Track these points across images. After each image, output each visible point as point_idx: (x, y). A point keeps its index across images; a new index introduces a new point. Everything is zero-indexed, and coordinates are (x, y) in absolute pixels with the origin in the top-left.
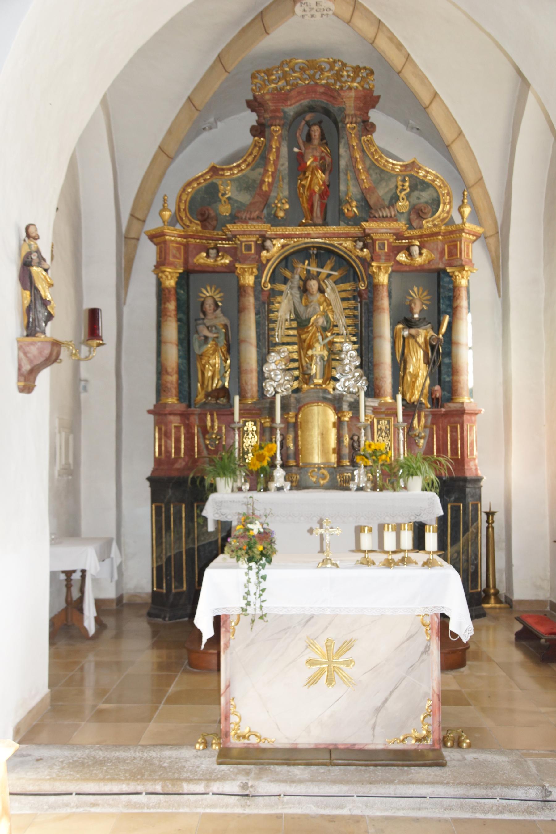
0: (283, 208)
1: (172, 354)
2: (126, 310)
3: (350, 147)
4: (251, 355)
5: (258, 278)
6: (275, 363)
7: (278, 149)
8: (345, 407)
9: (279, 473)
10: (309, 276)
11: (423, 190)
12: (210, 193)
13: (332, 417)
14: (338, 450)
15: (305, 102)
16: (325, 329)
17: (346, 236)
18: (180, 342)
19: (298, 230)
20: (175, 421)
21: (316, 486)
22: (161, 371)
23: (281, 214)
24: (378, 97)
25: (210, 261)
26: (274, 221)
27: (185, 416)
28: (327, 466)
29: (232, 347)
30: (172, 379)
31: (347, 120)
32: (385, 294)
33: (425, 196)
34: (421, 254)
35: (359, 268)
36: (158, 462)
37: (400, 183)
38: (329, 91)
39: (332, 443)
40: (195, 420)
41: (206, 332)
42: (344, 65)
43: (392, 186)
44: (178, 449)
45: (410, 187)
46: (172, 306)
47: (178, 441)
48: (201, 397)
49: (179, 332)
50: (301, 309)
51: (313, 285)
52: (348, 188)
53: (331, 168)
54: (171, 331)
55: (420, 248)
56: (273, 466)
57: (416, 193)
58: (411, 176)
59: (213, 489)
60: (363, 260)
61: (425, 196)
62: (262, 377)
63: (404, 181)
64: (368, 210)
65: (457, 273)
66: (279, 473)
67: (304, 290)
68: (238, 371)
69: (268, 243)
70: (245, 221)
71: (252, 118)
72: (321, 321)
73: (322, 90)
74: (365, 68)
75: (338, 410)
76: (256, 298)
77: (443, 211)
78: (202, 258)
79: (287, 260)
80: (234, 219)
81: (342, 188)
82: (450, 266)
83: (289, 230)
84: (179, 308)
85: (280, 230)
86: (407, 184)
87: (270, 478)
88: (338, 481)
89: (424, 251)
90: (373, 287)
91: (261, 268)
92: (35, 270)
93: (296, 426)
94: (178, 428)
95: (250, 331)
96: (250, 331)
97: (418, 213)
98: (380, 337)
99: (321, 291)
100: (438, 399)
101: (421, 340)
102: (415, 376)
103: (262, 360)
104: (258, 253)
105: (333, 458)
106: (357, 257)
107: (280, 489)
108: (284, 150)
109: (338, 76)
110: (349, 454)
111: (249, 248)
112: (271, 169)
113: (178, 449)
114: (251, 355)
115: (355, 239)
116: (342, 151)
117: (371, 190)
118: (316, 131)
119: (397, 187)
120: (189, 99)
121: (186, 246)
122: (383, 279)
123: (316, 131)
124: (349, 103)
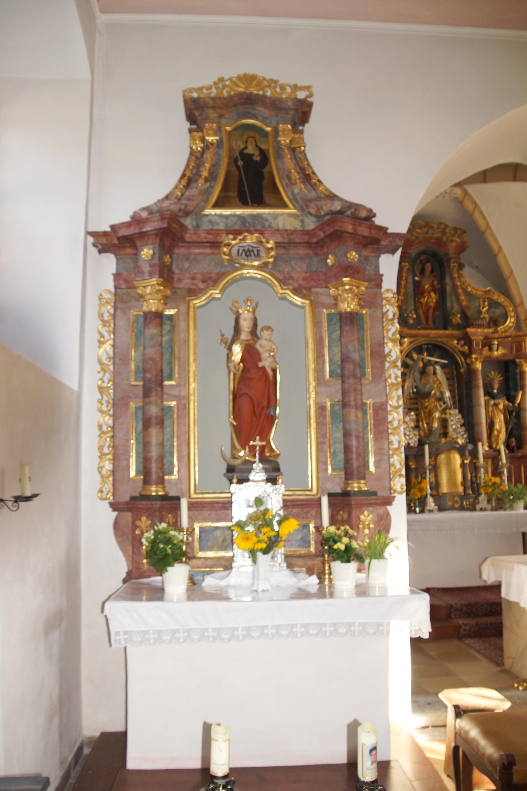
3: (452, 278)
7: (407, 278)
9: (430, 501)
11: (496, 308)
14: (464, 483)
15: (422, 248)
17: (453, 337)
21: (453, 509)
23: (411, 321)
24: (468, 247)
31: (452, 261)
32: (480, 376)
33: (498, 312)
34: (497, 350)
35: (460, 359)
37: (482, 303)
38: (439, 242)
42: (446, 226)
43: (477, 304)
45: (488, 305)
50: (421, 386)
52: (452, 304)
55: (498, 345)
57: (492, 310)
58: (489, 299)
60: (463, 353)
61: (498, 312)
63: (484, 301)
65: (523, 363)
66: (430, 501)
73: (434, 241)
74: (460, 229)
77: (510, 322)
81: (449, 304)
82: (519, 358)
83: (415, 332)
86: (486, 304)
89: (500, 348)
97: (495, 322)
100: (513, 447)
101: (501, 407)
102: (499, 432)
105: (461, 489)
106: (459, 351)
107: (430, 511)
108: (410, 279)
109: (443, 232)
110: (472, 487)
117: (468, 307)
118: (428, 267)
119: (480, 305)
122: (479, 366)
123: (428, 267)
124: (451, 249)
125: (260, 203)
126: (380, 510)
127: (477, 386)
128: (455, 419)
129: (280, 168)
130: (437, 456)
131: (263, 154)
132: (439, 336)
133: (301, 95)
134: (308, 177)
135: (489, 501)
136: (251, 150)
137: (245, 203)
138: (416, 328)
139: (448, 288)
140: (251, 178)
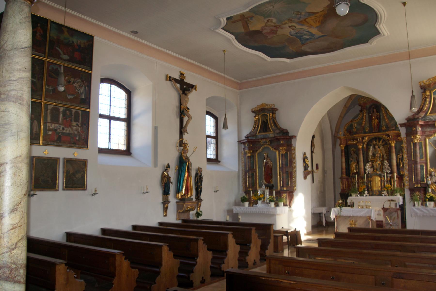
0: (367, 129)
1: (344, 165)
2: (335, 153)
3: (383, 113)
4: (362, 164)
5: (363, 146)
6: (368, 166)
8: (382, 176)
10: (376, 144)
12: (351, 126)
13: (379, 179)
16: (380, 157)
17: (384, 134)
18: (346, 161)
19: (372, 134)
20: (345, 180)
21: (376, 195)
22: (342, 169)
23: (367, 131)
25: (352, 143)
26: (365, 133)
27: (347, 179)
28: (378, 191)
29: (358, 162)
30: (344, 170)
36: (342, 190)
39: (379, 185)
40: (350, 180)
41: (351, 159)
44: (346, 187)
46: (343, 154)
47: (346, 185)
48: (351, 175)
49: (346, 159)
51: (377, 147)
52: (383, 123)
53: (379, 118)
54: (344, 159)
56: (365, 191)
59: (351, 196)
62: (365, 170)
64: (388, 129)
66: (366, 192)
67: (374, 148)
68: (359, 168)
69: (365, 138)
70: (358, 133)
71: (360, 108)
72: (379, 155)
75: (381, 177)
76: (363, 151)
78: (350, 142)
79: (370, 141)
80: (356, 133)
81: (382, 123)
83: (369, 134)
84: (345, 154)
85: (367, 135)
87: (364, 193)
88: (380, 194)
90: (391, 146)
91: (363, 144)
92: (306, 160)
93: (371, 181)
94: (346, 182)
95: (361, 159)
96: (361, 159)
98: (393, 159)
99: (379, 148)
103: (365, 165)
104: (363, 141)
105: (380, 189)
107: (367, 196)
108: (367, 116)
110: (383, 187)
111: (360, 139)
112: (364, 120)
113: (346, 187)
114: (362, 164)
115: (386, 135)
116: (381, 114)
118: (375, 110)
120: (345, 105)
121: (346, 139)
125: (266, 131)
126: (291, 194)
127: (393, 152)
128: (386, 163)
129: (271, 124)
130: (371, 177)
131: (267, 120)
132: (380, 134)
133: (273, 107)
134: (275, 124)
135: (388, 193)
136: (265, 120)
137: (264, 132)
138: (370, 133)
139: (381, 117)
140: (265, 127)
